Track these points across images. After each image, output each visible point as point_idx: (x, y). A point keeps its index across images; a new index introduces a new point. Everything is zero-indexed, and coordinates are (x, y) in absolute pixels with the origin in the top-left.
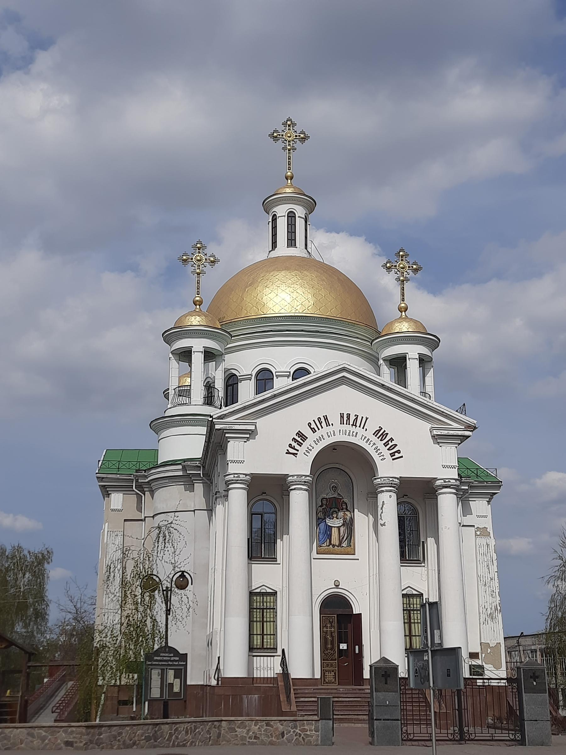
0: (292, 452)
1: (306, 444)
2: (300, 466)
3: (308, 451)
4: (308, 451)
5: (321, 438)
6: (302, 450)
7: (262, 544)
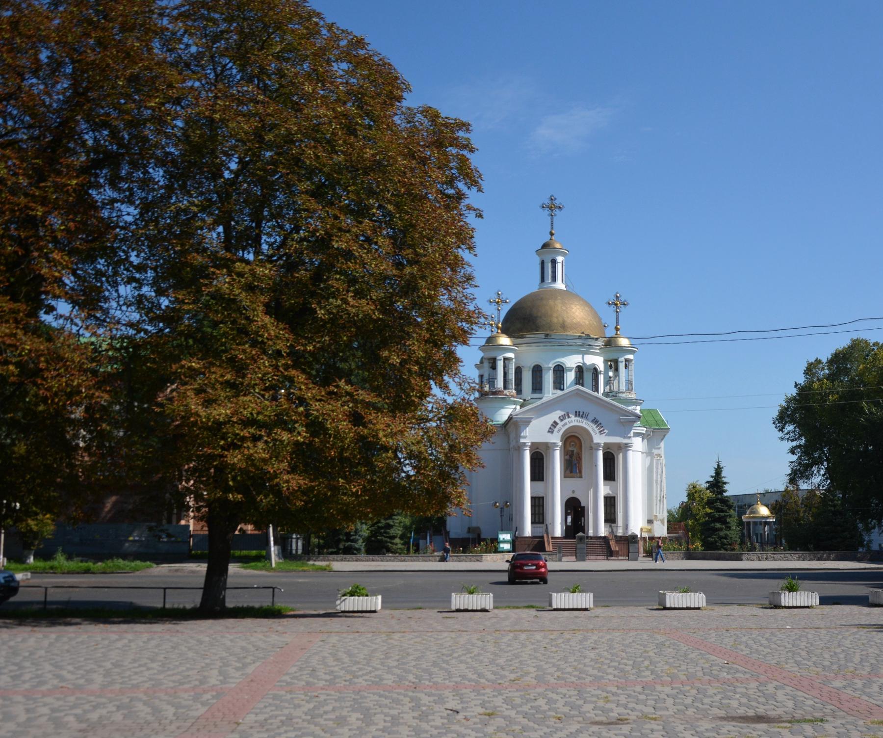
0: (551, 431)
1: (558, 427)
2: (556, 439)
3: (559, 430)
4: (559, 430)
5: (566, 424)
6: (556, 430)
7: (538, 474)
